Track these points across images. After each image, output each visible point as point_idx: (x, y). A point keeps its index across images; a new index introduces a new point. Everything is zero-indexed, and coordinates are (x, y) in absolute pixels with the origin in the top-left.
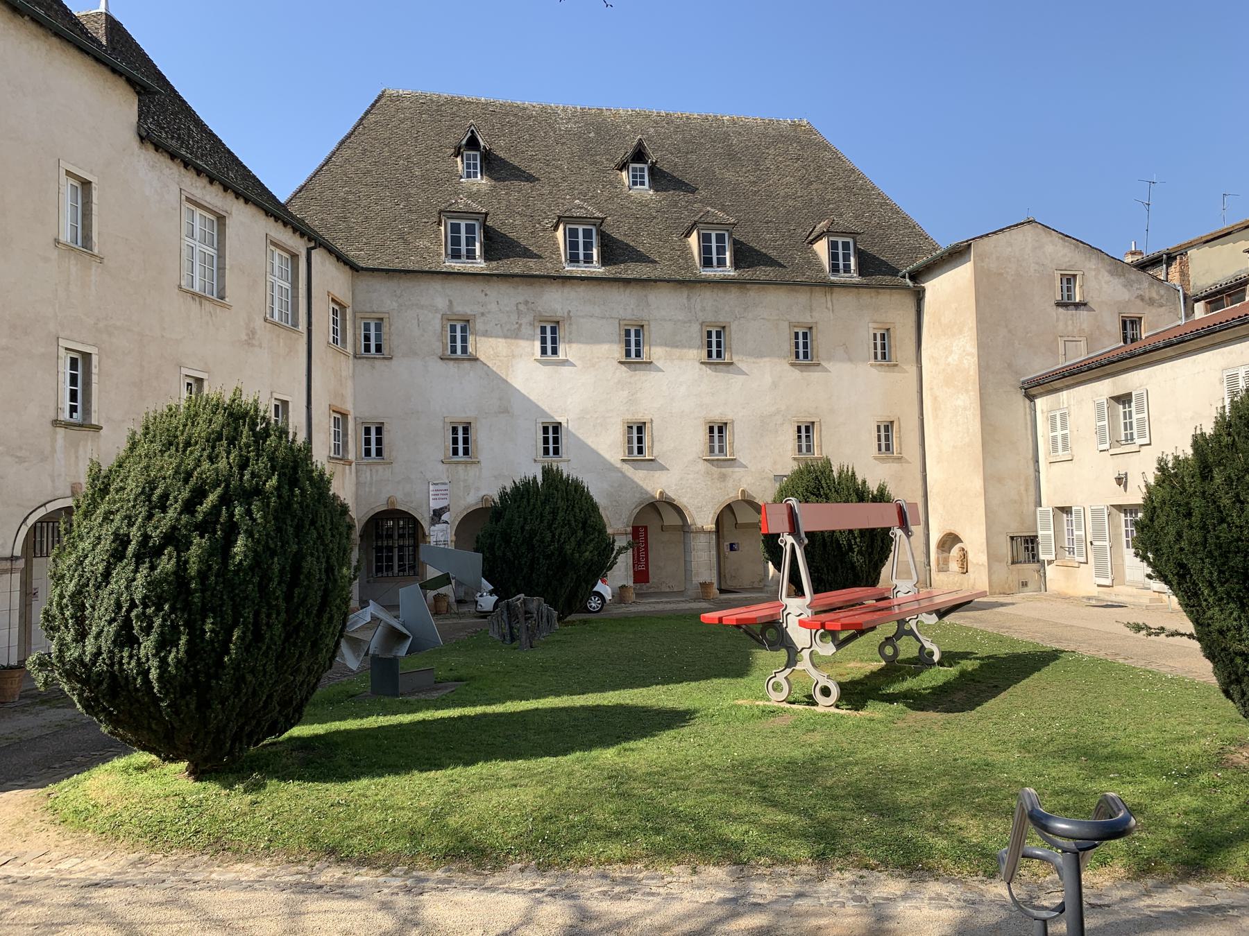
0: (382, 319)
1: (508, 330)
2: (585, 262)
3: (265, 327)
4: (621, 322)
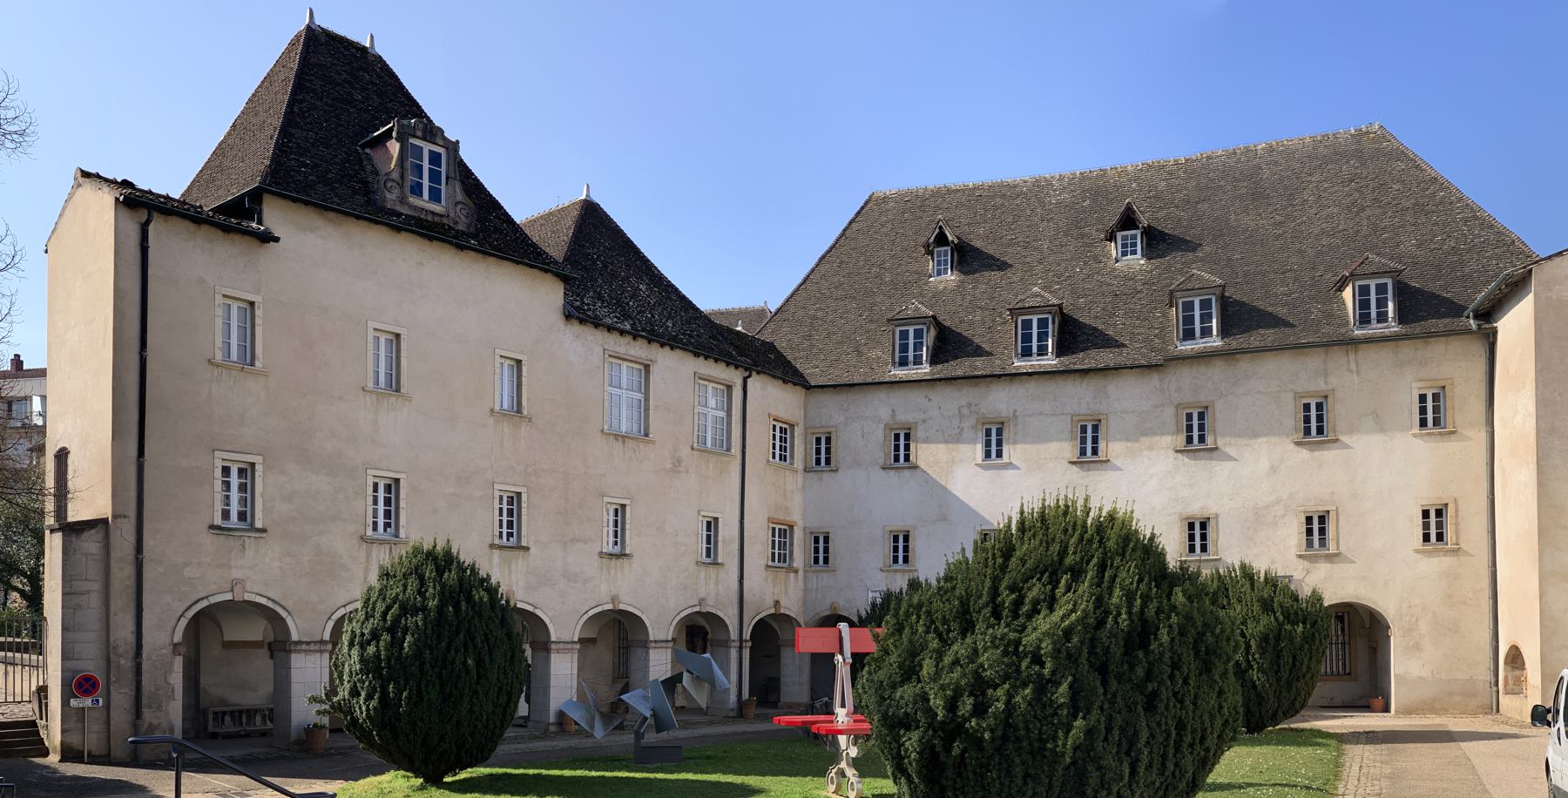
0: (830, 433)
1: (950, 435)
2: (1038, 355)
3: (692, 455)
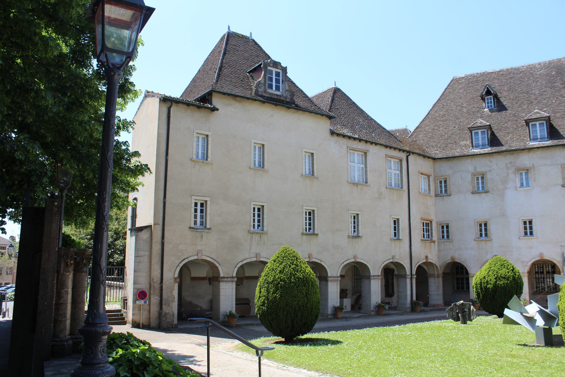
0: (446, 178)
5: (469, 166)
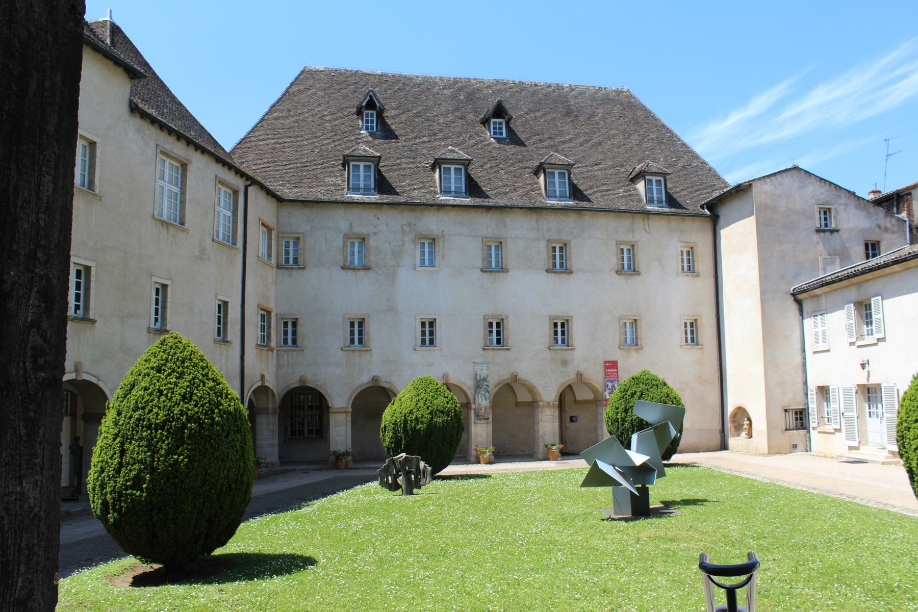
0: (298, 238)
4: (484, 239)
5: (341, 220)
